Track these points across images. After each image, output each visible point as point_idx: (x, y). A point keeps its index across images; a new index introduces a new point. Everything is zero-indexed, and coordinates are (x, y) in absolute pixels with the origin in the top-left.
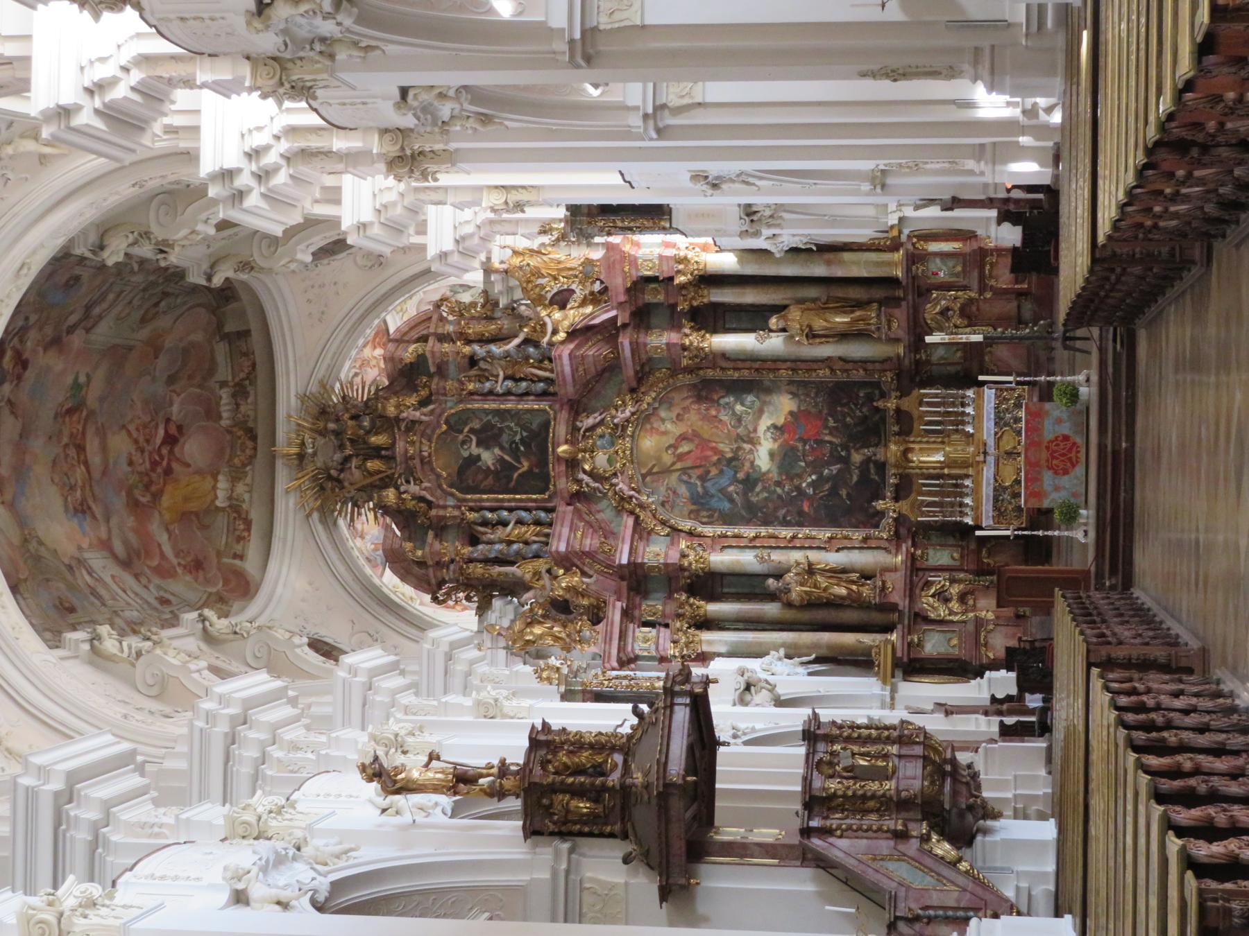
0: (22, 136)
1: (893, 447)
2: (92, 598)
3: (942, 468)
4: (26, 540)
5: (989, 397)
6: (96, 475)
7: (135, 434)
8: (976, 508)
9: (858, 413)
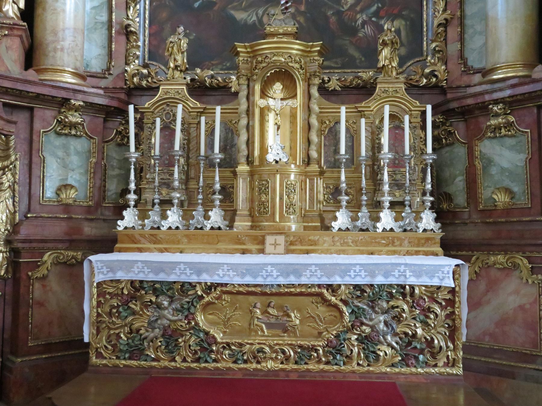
1: (296, 47)
3: (249, 161)
5: (432, 271)
8: (156, 239)
9: (361, 18)
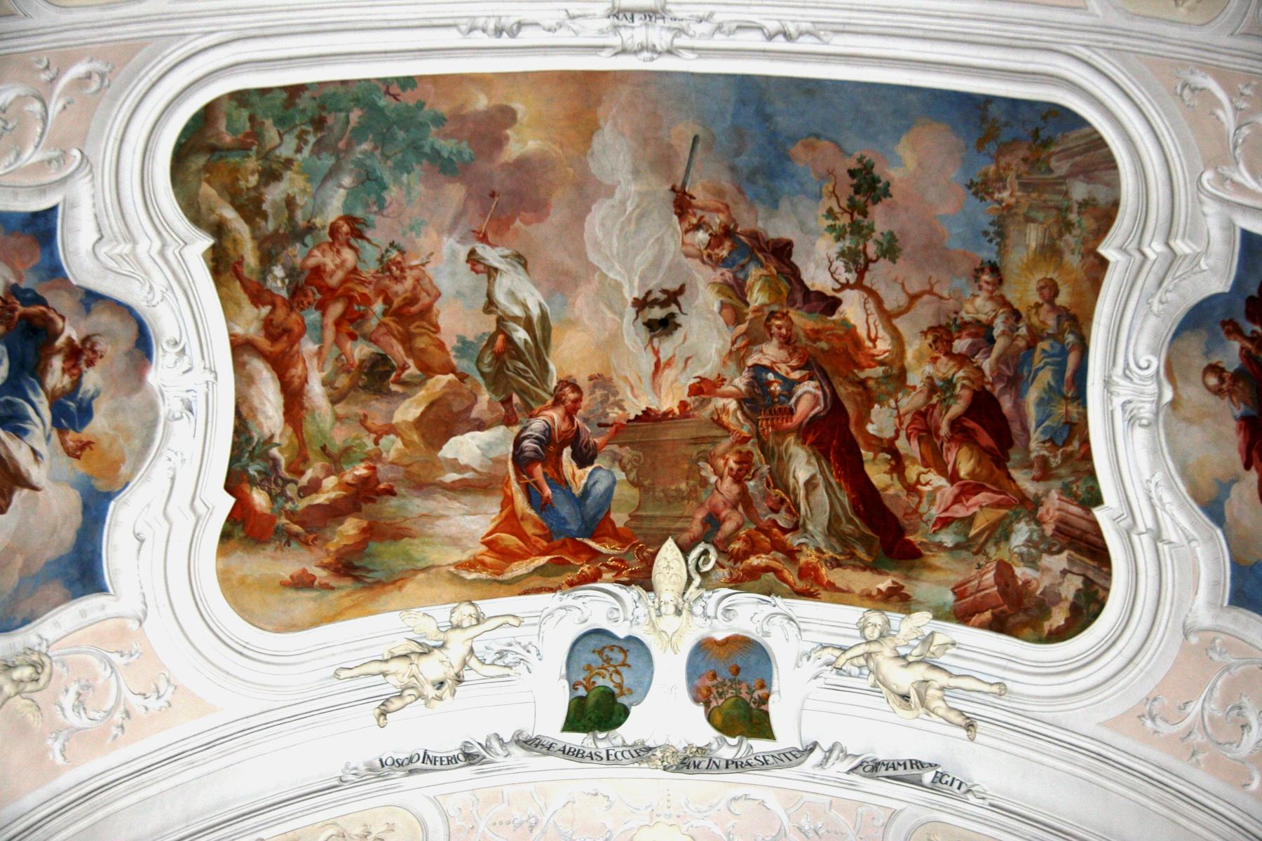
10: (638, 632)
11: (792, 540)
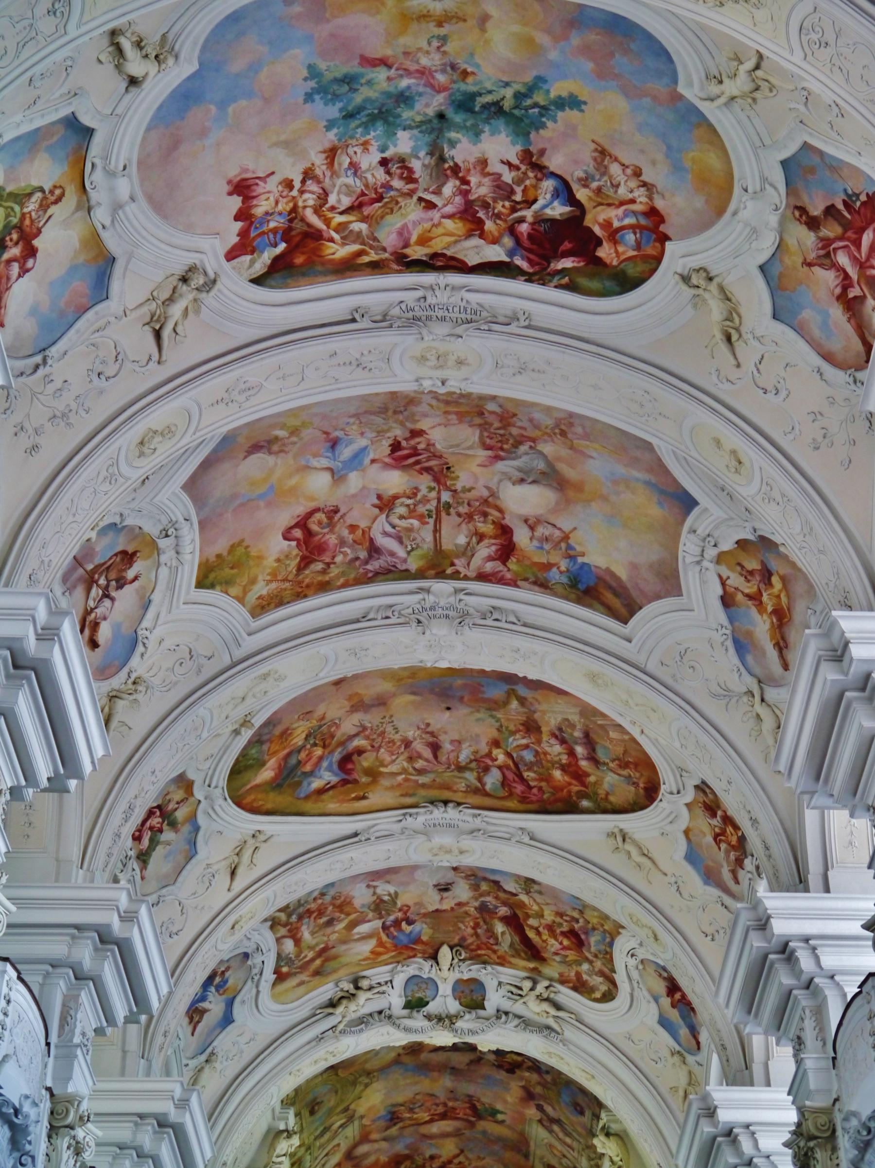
0: (690, 1073)
2: (321, 1128)
4: (368, 1074)
6: (424, 1130)
7: (456, 1161)
10: (433, 976)
11: (496, 947)
